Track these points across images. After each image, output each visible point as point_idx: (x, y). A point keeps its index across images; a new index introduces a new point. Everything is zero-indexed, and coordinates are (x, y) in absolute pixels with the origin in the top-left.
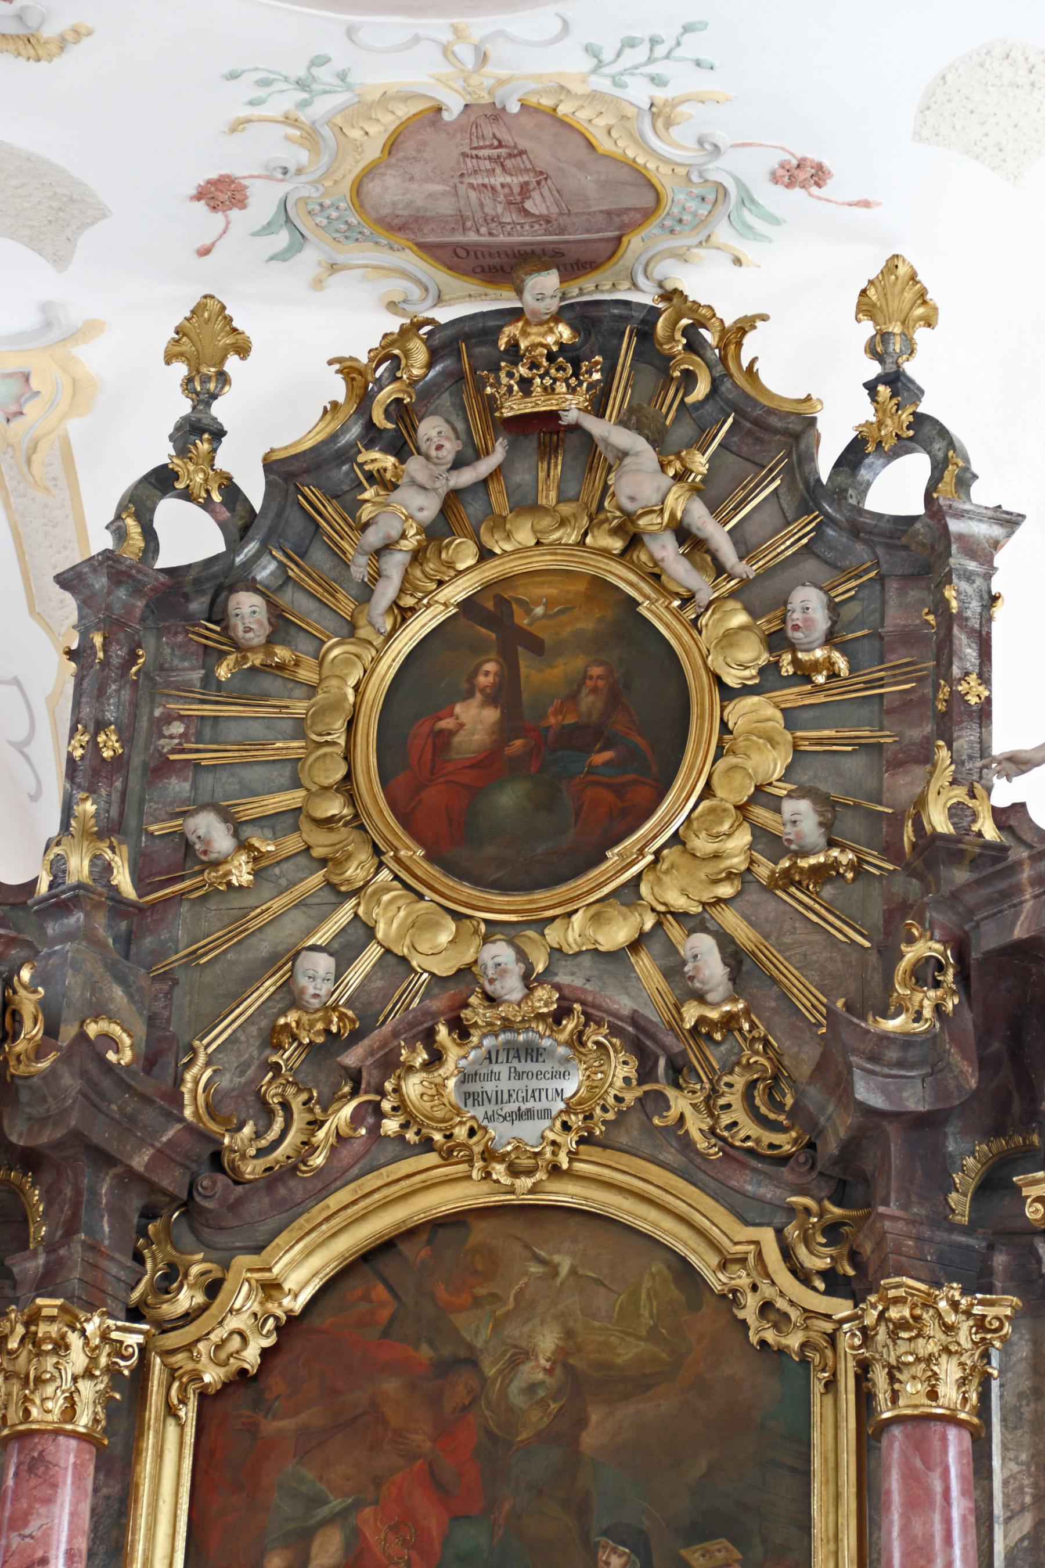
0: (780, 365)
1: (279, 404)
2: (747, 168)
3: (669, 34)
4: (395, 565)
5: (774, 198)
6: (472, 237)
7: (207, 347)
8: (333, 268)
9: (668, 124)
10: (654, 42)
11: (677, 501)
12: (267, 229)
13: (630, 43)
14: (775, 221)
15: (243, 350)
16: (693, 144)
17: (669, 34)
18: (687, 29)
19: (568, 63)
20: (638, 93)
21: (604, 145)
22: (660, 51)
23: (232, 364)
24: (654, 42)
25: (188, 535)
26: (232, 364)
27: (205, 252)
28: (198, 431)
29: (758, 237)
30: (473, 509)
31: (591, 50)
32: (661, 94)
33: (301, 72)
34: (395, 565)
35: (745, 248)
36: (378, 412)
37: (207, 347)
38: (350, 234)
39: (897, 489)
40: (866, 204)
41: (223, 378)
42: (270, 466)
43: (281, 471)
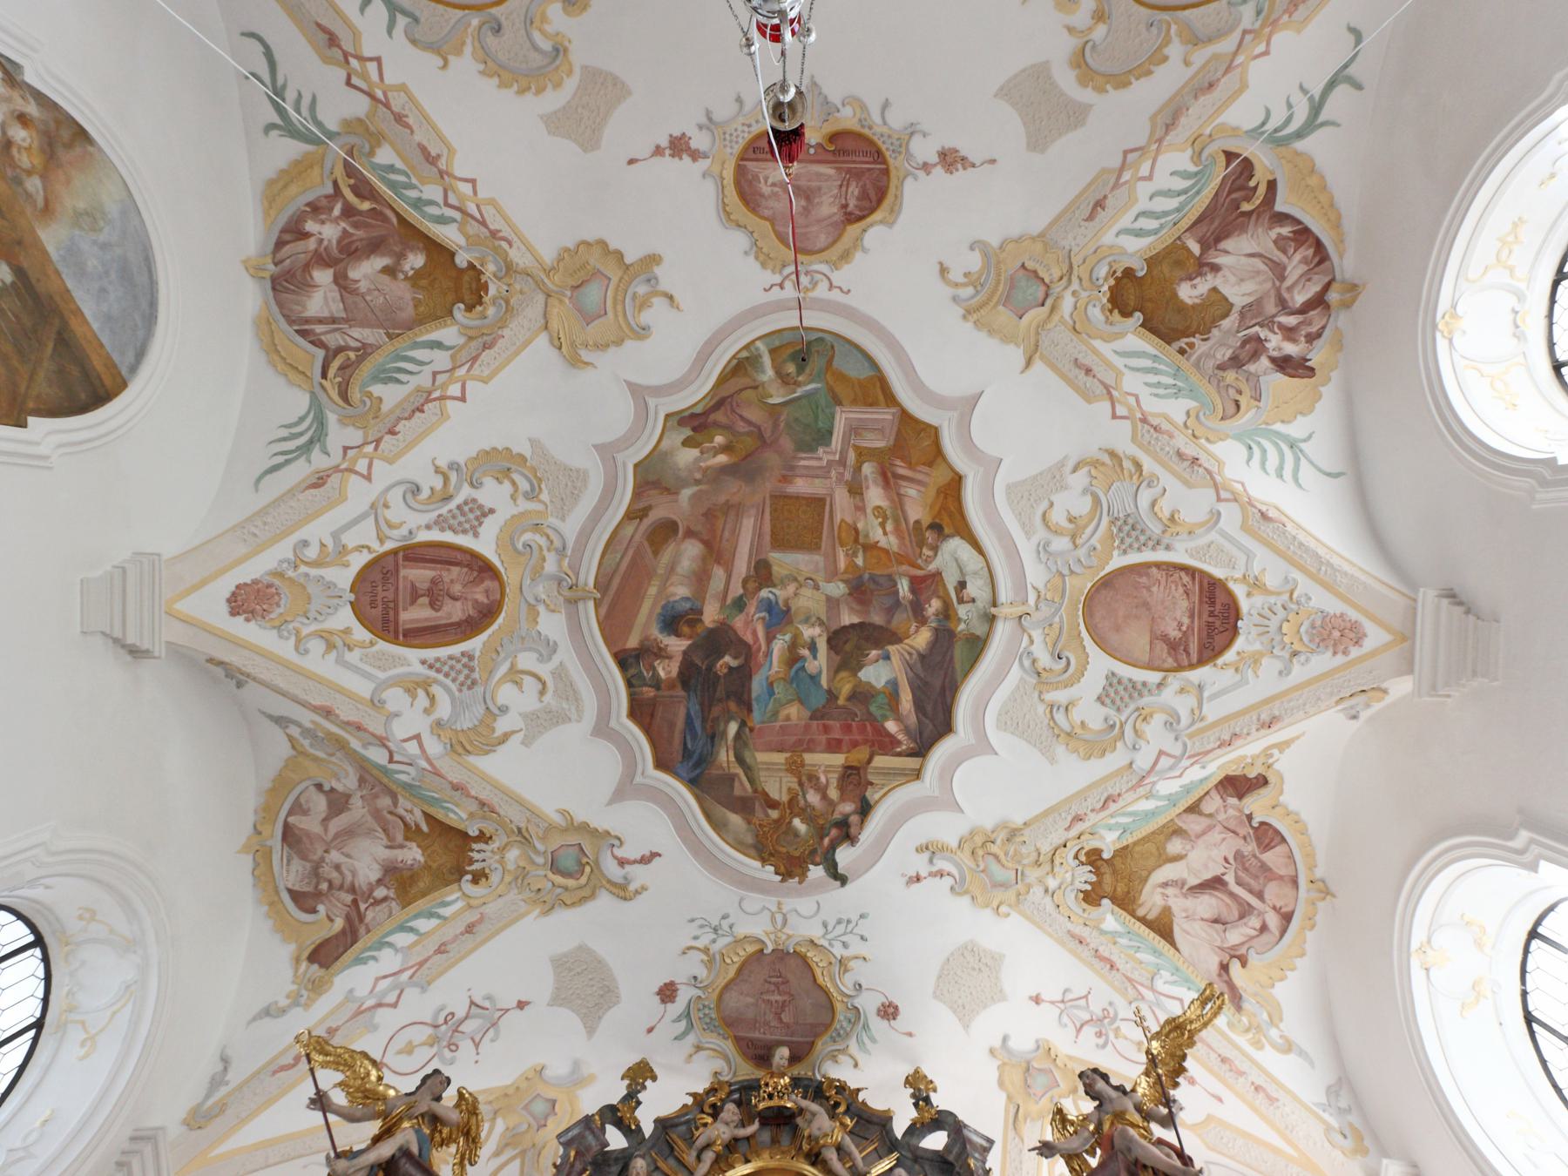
0: (875, 1101)
1: (661, 1101)
2: (868, 1004)
3: (854, 918)
4: (709, 1156)
5: (877, 1024)
6: (757, 1035)
7: (639, 1075)
8: (699, 1048)
9: (846, 971)
10: (849, 922)
11: (839, 1135)
12: (678, 1020)
13: (839, 922)
14: (873, 1040)
15: (654, 1078)
16: (851, 986)
17: (854, 918)
18: (862, 916)
19: (816, 932)
20: (838, 951)
21: (820, 980)
22: (850, 927)
23: (648, 1083)
24: (849, 922)
25: (616, 1140)
26: (648, 1083)
27: (650, 1030)
28: (632, 1098)
29: (867, 1052)
30: (743, 1147)
31: (825, 925)
32: (846, 953)
33: (715, 923)
34: (709, 1156)
35: (860, 1057)
36: (706, 1105)
37: (639, 1075)
38: (709, 1027)
39: (936, 1141)
40: (910, 1035)
41: (644, 1088)
42: (658, 1121)
43: (663, 1124)
